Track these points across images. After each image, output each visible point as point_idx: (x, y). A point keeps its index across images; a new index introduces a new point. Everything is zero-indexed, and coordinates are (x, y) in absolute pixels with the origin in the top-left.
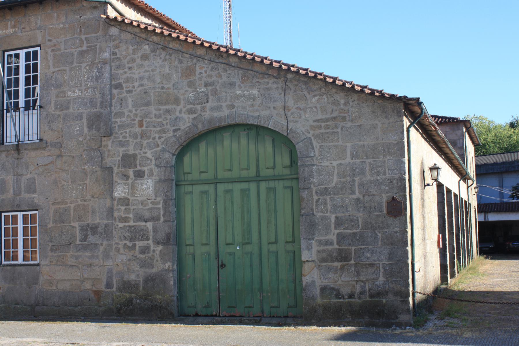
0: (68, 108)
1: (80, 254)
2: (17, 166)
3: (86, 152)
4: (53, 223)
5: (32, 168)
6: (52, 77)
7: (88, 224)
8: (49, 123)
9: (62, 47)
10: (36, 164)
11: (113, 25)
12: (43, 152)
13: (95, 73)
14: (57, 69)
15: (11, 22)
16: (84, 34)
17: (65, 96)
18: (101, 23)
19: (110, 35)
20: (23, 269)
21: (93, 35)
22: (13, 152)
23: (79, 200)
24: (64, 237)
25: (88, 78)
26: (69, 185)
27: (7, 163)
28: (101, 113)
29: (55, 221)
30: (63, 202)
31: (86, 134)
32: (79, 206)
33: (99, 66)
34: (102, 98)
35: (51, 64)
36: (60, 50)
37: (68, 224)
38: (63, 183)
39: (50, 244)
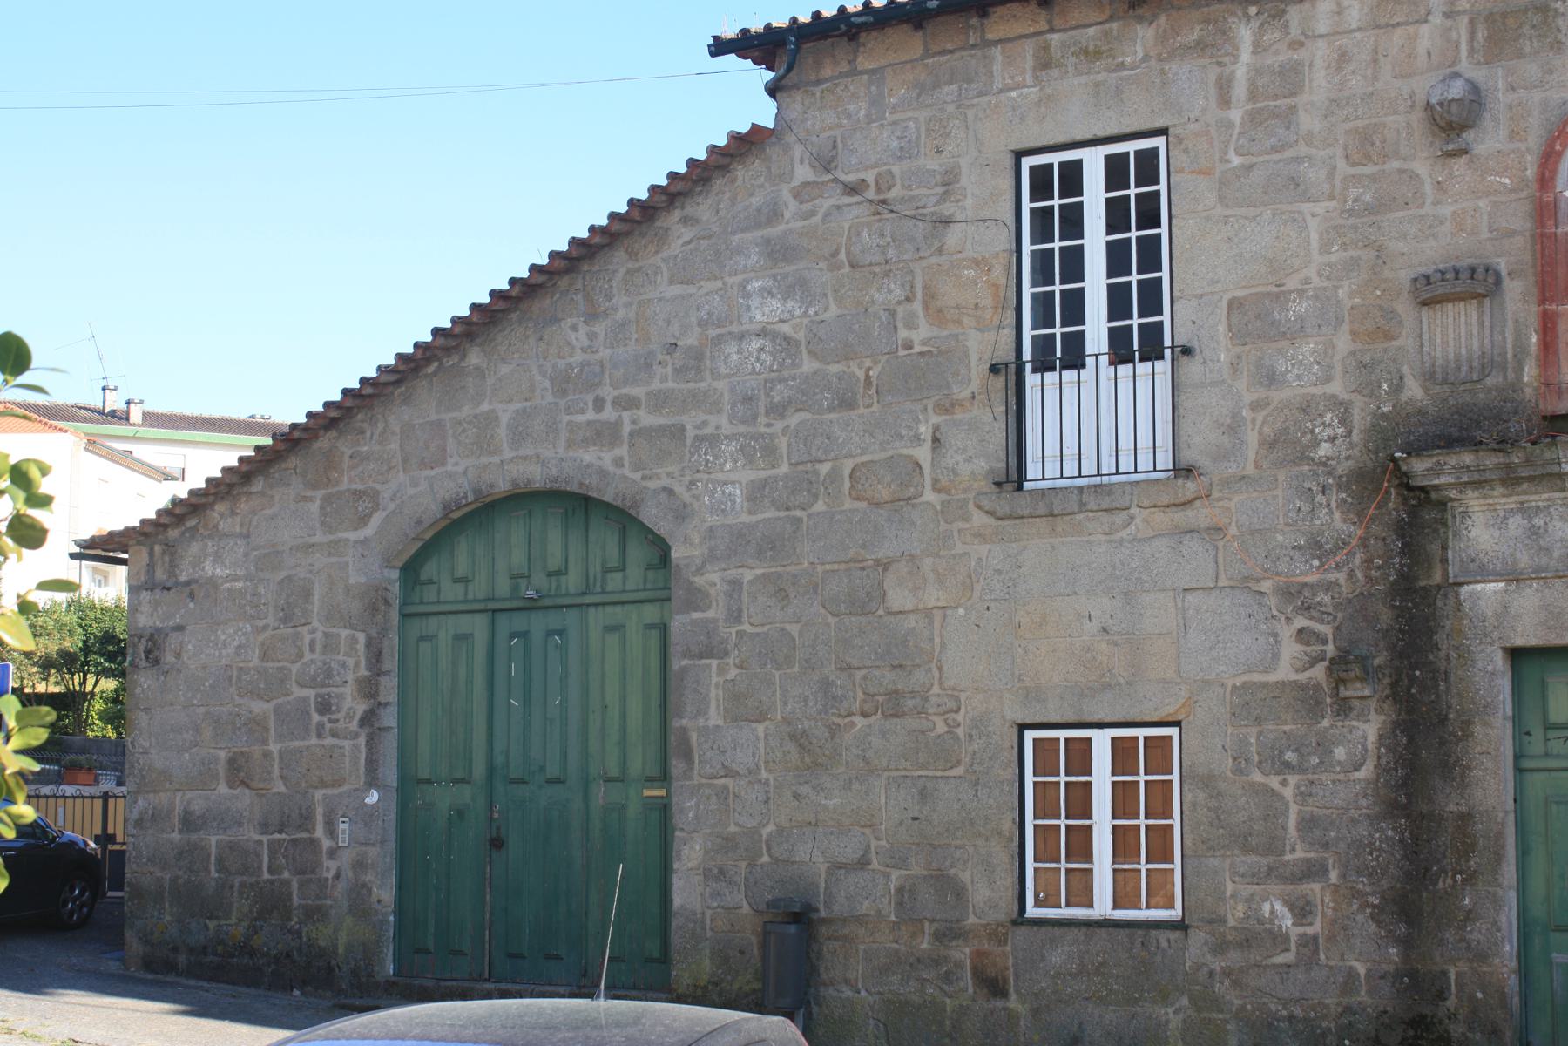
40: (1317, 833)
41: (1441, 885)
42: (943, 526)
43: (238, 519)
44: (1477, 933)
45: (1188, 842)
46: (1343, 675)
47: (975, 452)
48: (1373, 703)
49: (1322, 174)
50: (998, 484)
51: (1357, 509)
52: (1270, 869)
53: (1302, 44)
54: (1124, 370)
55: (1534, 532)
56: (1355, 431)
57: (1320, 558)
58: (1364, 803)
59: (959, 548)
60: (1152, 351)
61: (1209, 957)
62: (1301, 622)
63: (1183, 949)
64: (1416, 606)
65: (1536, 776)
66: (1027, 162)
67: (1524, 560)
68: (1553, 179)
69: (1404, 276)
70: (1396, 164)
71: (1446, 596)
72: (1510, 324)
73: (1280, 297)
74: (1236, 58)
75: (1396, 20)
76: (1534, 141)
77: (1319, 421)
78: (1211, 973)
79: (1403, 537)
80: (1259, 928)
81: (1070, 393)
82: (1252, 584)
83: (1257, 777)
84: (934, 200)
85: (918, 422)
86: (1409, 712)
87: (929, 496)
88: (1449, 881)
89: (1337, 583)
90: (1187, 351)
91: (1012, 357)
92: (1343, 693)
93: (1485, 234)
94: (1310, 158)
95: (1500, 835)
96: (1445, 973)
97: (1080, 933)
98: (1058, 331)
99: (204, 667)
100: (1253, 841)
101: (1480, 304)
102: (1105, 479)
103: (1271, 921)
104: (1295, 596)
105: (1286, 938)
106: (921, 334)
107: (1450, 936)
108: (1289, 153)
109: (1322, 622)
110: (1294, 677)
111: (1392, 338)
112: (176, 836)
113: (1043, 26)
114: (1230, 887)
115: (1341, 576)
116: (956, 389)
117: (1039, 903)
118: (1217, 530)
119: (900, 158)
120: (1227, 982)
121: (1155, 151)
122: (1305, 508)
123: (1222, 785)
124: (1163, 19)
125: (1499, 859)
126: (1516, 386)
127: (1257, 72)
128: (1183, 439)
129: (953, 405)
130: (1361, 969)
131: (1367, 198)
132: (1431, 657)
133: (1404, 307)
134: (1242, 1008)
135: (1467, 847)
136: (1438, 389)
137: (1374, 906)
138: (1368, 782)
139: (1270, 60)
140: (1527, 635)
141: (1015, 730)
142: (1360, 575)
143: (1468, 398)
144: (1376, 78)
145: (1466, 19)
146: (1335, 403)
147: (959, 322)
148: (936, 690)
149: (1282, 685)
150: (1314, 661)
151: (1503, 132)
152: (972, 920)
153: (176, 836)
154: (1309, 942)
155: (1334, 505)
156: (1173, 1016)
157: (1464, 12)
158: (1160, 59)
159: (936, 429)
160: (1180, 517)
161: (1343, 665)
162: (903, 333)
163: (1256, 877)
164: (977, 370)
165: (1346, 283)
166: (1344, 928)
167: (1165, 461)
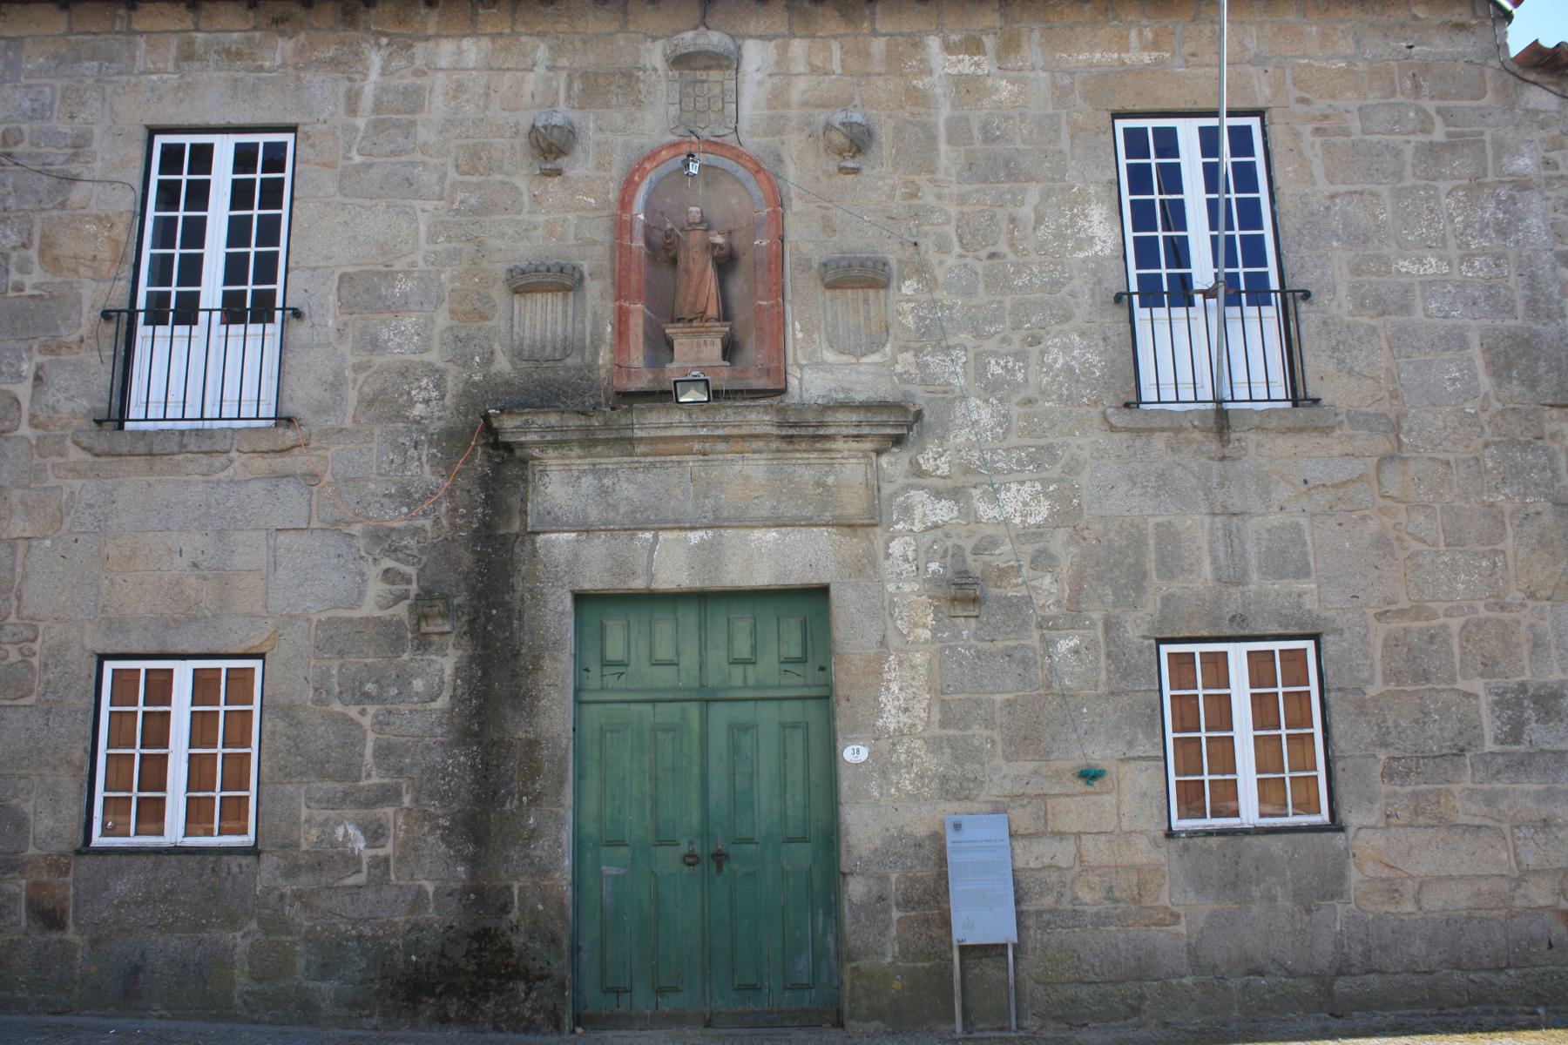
0: (1406, 309)
1: (1498, 786)
2: (1221, 485)
3: (1492, 449)
4: (1386, 682)
5: (1282, 493)
6: (1328, 208)
7: (1523, 687)
8: (1334, 349)
9: (1355, 125)
10: (1299, 482)
11: (1535, 83)
12: (1324, 441)
13: (1490, 211)
14: (1342, 188)
15: (1140, 33)
16: (1432, 98)
17: (1388, 272)
18: (1489, 72)
19: (1527, 111)
20: (1276, 844)
21: (1465, 103)
22: (1197, 435)
23: (1480, 605)
24: (1432, 729)
25: (1467, 225)
26: (1438, 554)
27: (1178, 471)
28: (1535, 334)
29: (1392, 675)
30: (1418, 612)
31: (1486, 396)
32: (1480, 624)
33: (1503, 193)
34: (1532, 287)
35: (1318, 168)
36: (1346, 132)
37: (1443, 686)
38: (1415, 546)
39: (1382, 755)
40: (393, 759)
41: (508, 806)
42: (37, 460)
44: (540, 850)
45: (265, 769)
46: (427, 610)
47: (78, 389)
48: (451, 639)
49: (434, 178)
50: (99, 422)
51: (446, 465)
52: (346, 794)
53: (425, 74)
54: (236, 330)
55: (603, 491)
56: (448, 396)
57: (408, 506)
58: (439, 731)
59: (52, 481)
60: (263, 310)
61: (280, 881)
62: (387, 563)
63: (255, 875)
64: (495, 551)
65: (593, 707)
66: (160, 140)
67: (594, 515)
68: (631, 203)
69: (500, 269)
70: (499, 177)
71: (523, 543)
72: (589, 315)
73: (389, 276)
74: (365, 76)
75: (507, 65)
76: (616, 173)
77: (416, 384)
78: (282, 897)
79: (486, 490)
80: (331, 851)
81: (180, 346)
82: (343, 527)
83: (337, 707)
84: (62, 159)
85: (20, 359)
86: (483, 647)
87: (25, 430)
88: (516, 803)
89: (423, 529)
90: (297, 314)
91: (126, 306)
92: (425, 628)
93: (572, 241)
94: (424, 164)
95: (563, 759)
96: (509, 888)
97: (149, 861)
98: (174, 289)
100: (330, 768)
101: (565, 297)
102: (207, 424)
103: (344, 844)
104: (381, 538)
105: (358, 860)
106: (35, 278)
107: (514, 853)
108: (405, 158)
109: (407, 563)
110: (377, 613)
111: (487, 319)
113: (189, 24)
114: (304, 813)
115: (427, 523)
116: (64, 332)
117: (106, 832)
118: (312, 478)
119: (31, 118)
120: (297, 904)
121: (283, 146)
122: (398, 460)
123: (302, 715)
124: (302, 36)
125: (561, 781)
126: (592, 367)
127: (384, 89)
128: (287, 392)
129: (59, 347)
130: (430, 888)
131: (473, 201)
132: (507, 598)
133: (499, 294)
134: (312, 929)
135: (532, 770)
136: (525, 364)
137: (445, 828)
138: (443, 711)
139: (395, 82)
140: (593, 581)
141: (95, 660)
142: (445, 522)
143: (550, 374)
144: (486, 108)
145: (564, 74)
146: (431, 370)
147: (76, 271)
148: (13, 618)
149: (366, 620)
150: (398, 599)
151: (591, 163)
152: (31, 850)
154: (381, 864)
155: (424, 459)
156: (240, 941)
157: (564, 68)
158: (296, 67)
159: (40, 367)
160: (277, 462)
161: (427, 602)
162: (15, 276)
163: (331, 803)
164: (89, 317)
165: (448, 270)
166: (416, 849)
167: (268, 410)
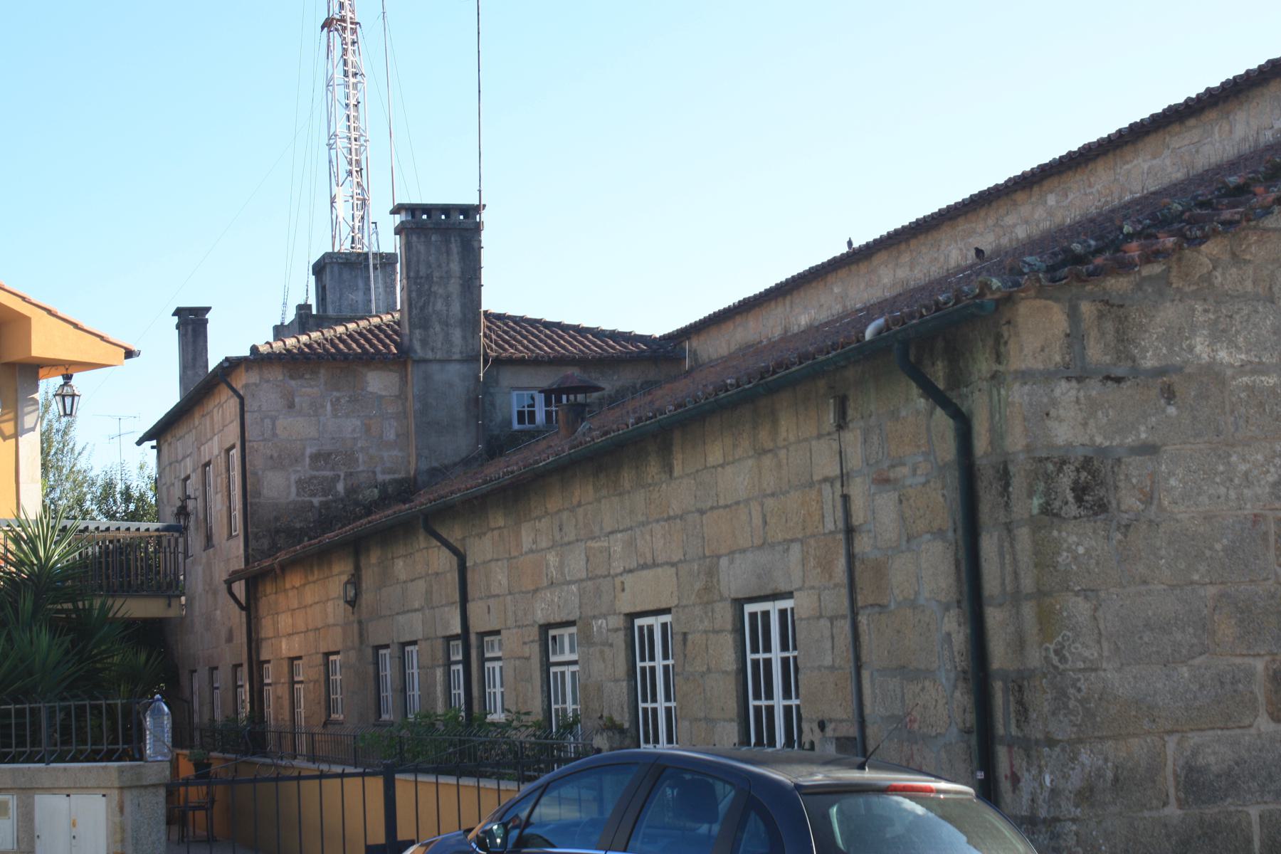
43: (1250, 270)
99: (1208, 518)
112: (1173, 811)
153: (1173, 811)
